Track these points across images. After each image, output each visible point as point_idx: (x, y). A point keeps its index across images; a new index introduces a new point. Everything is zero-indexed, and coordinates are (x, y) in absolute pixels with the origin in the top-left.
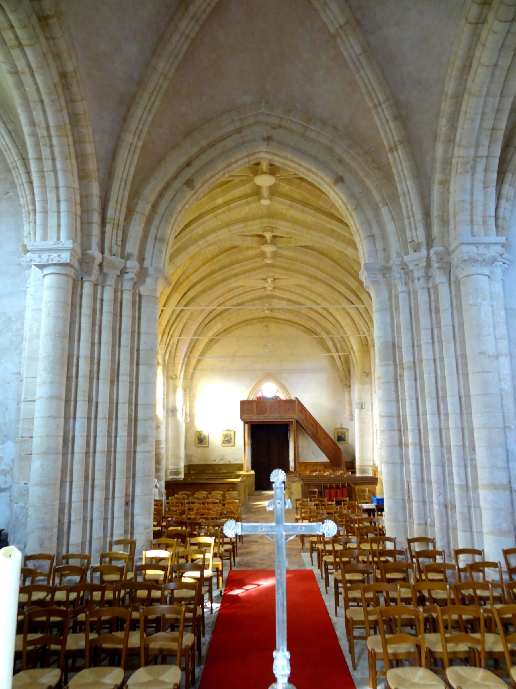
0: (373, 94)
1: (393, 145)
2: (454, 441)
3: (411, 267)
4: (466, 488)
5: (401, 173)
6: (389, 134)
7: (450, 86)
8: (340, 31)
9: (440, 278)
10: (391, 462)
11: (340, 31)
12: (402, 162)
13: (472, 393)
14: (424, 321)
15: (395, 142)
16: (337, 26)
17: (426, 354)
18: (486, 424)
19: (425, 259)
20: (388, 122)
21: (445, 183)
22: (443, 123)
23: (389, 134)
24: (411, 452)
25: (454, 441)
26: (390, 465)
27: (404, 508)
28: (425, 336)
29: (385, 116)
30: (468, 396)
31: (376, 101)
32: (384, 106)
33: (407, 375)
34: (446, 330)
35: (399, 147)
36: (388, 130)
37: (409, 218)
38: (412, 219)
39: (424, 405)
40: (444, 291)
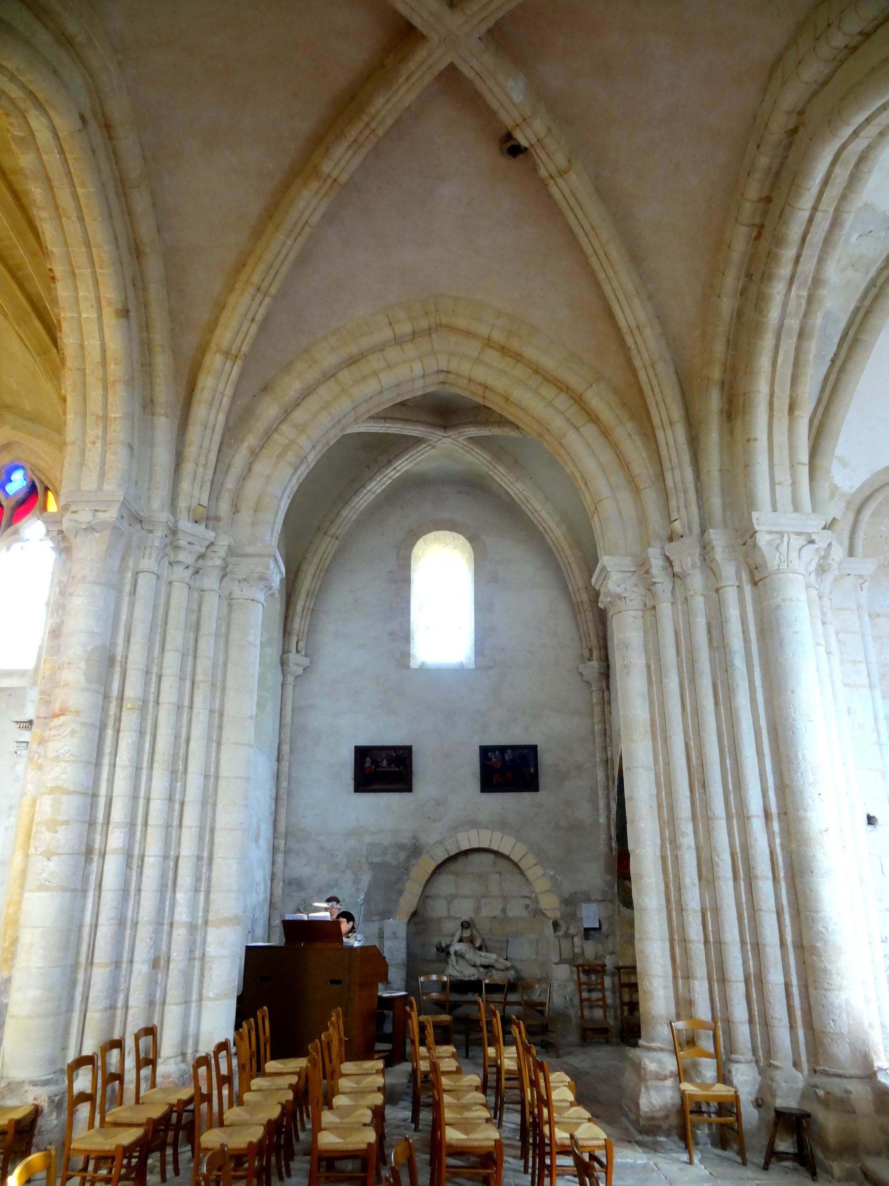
0: (272, 272)
1: (234, 352)
2: (188, 849)
3: (183, 543)
4: (192, 928)
5: (218, 396)
6: (241, 335)
7: (329, 360)
8: (329, 181)
9: (210, 581)
10: (72, 887)
11: (329, 181)
12: (229, 384)
13: (223, 773)
14: (176, 637)
15: (240, 351)
16: (334, 175)
17: (168, 695)
18: (241, 823)
19: (207, 543)
20: (253, 320)
21: (255, 454)
22: (293, 386)
23: (241, 335)
24: (112, 867)
25: (188, 849)
26: (69, 894)
27: (73, 984)
28: (171, 660)
29: (257, 311)
30: (217, 778)
31: (266, 284)
32: (268, 300)
33: (129, 720)
34: (204, 664)
35: (239, 362)
36: (244, 329)
37: (197, 465)
38: (200, 469)
39: (150, 779)
40: (212, 605)
